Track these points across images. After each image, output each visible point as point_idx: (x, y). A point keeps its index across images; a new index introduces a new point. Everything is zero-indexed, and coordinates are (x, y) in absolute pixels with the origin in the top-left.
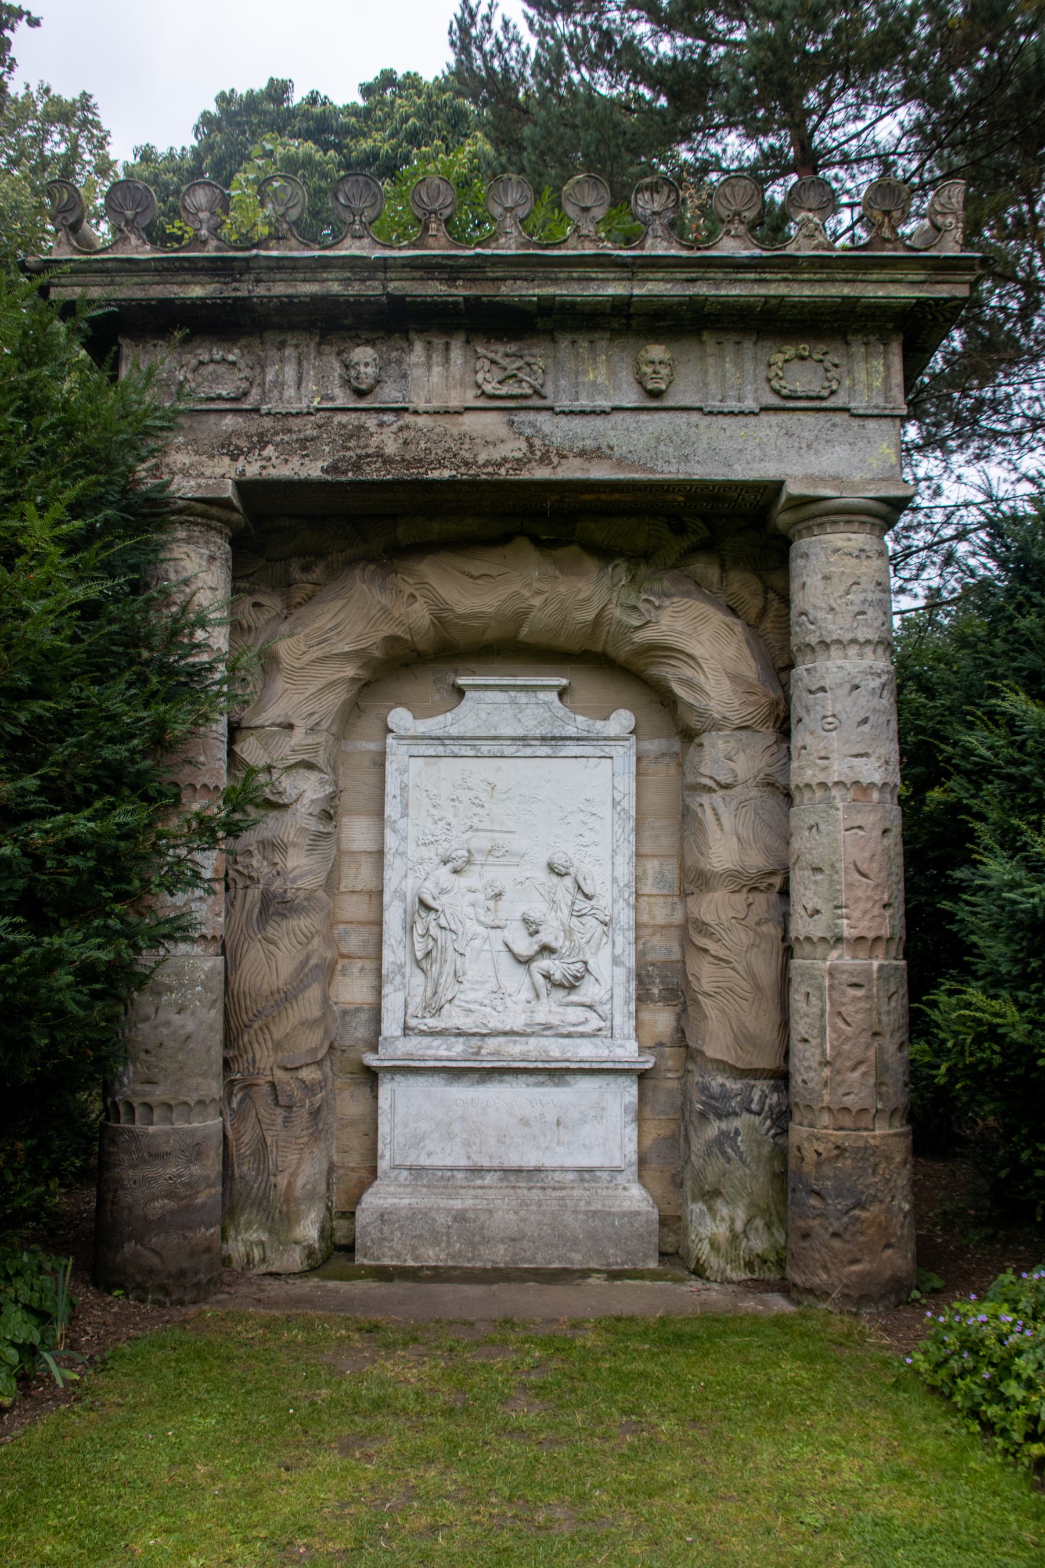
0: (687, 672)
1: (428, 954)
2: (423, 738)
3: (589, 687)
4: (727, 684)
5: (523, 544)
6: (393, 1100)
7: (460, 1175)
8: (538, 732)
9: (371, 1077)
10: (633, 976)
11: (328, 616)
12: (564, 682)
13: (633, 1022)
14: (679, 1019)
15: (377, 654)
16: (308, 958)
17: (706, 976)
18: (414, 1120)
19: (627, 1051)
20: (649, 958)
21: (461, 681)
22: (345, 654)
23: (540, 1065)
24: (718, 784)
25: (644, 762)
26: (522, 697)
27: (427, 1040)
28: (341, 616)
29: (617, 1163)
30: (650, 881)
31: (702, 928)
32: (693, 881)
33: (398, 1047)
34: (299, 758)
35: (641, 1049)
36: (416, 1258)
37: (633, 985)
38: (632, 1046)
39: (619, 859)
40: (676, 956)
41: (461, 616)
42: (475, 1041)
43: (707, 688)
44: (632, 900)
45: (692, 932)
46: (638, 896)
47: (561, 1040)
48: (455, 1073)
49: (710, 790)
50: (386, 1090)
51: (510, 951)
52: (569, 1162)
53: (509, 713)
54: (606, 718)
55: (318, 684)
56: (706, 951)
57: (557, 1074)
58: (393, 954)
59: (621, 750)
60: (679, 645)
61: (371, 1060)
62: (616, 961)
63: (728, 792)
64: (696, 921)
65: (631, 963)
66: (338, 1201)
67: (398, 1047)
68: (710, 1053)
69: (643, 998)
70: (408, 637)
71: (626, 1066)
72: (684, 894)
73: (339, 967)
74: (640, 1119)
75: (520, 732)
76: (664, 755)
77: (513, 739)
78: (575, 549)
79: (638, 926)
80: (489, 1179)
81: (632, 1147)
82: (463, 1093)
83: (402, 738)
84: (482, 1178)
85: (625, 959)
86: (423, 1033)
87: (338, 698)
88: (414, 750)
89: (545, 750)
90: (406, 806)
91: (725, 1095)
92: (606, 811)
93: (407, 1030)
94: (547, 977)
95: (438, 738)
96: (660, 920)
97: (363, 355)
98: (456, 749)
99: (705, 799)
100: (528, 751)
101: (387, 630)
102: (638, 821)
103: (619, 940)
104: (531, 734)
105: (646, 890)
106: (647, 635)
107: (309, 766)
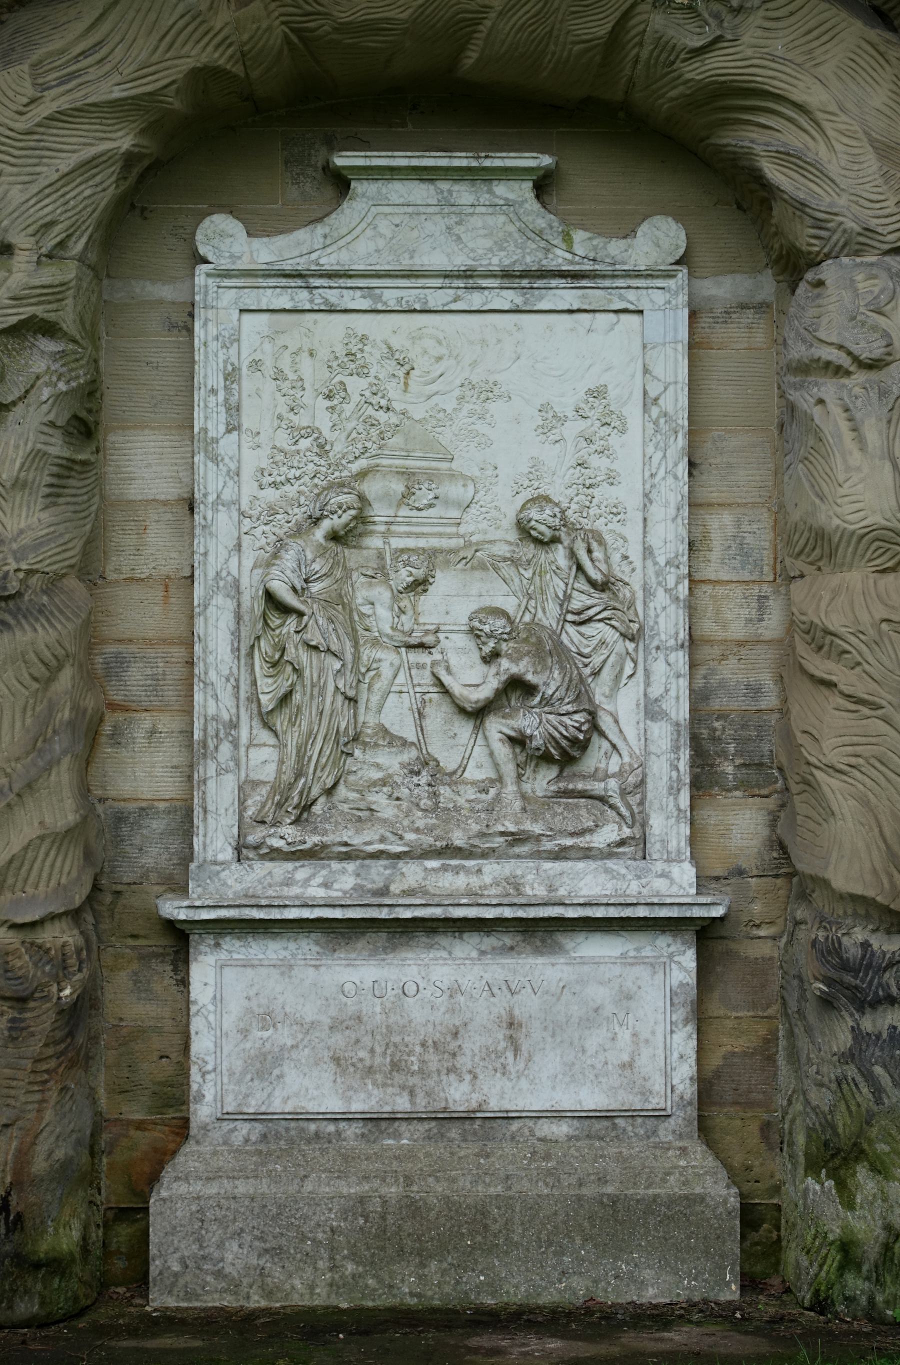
0: (792, 138)
1: (285, 698)
2: (267, 274)
4: (871, 163)
6: (219, 986)
7: (351, 1131)
8: (496, 262)
9: (179, 939)
10: (685, 739)
11: (80, 27)
12: (546, 160)
13: (686, 830)
14: (773, 823)
15: (176, 104)
16: (51, 709)
17: (831, 733)
19: (673, 883)
20: (716, 704)
21: (342, 160)
22: (114, 104)
23: (508, 913)
24: (856, 359)
25: (705, 321)
26: (464, 193)
27: (280, 869)
28: (105, 27)
29: (656, 1102)
30: (715, 555)
31: (821, 639)
32: (807, 548)
33: (224, 880)
34: (27, 312)
35: (703, 882)
36: (269, 1294)
37: (685, 755)
38: (685, 874)
39: (657, 512)
40: (770, 700)
41: (342, 28)
42: (378, 871)
43: (833, 169)
44: (683, 590)
45: (802, 648)
46: (694, 583)
47: (547, 865)
48: (339, 932)
49: (839, 371)
50: (205, 969)
51: (445, 691)
52: (566, 1100)
53: (436, 226)
54: (630, 233)
55: (65, 163)
56: (830, 685)
58: (215, 700)
59: (659, 297)
60: (778, 86)
61: (174, 909)
62: (651, 710)
63: (873, 375)
64: (810, 629)
65: (682, 711)
66: (110, 1192)
67: (224, 880)
68: (839, 883)
69: (703, 782)
70: (238, 70)
71: (674, 913)
72: (786, 578)
73: (107, 729)
74: (701, 1018)
75: (460, 261)
76: (743, 306)
77: (447, 275)
79: (694, 643)
80: (407, 1137)
81: (684, 1073)
83: (226, 274)
84: (397, 1136)
85: (668, 705)
86: (275, 855)
87: (102, 190)
88: (250, 299)
89: (507, 298)
90: (234, 409)
91: (869, 963)
94: (518, 741)
95: (299, 275)
96: (737, 630)
98: (333, 296)
99: (828, 388)
100: (476, 300)
101: (198, 55)
102: (695, 432)
103: (659, 668)
104: (483, 264)
105: (709, 572)
106: (717, 65)
107: (49, 329)
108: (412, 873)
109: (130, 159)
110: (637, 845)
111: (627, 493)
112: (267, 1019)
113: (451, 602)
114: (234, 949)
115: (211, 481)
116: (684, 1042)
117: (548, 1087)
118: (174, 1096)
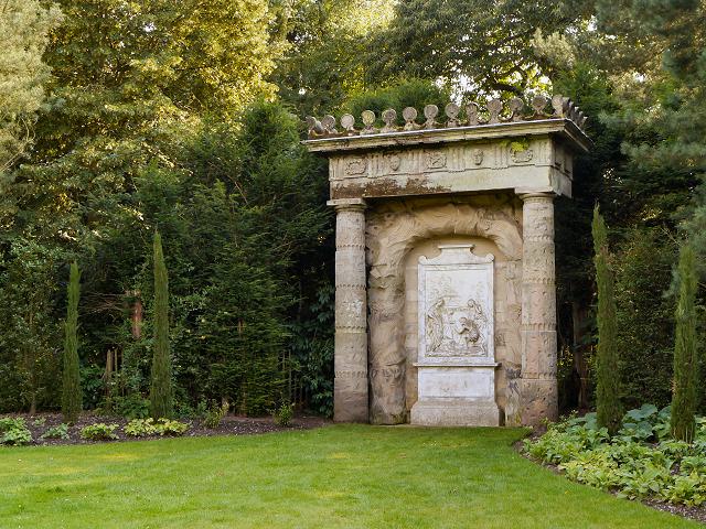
3: (480, 246)
5: (451, 205)
18: (428, 384)
26: (459, 251)
50: (420, 372)
52: (474, 394)
57: (470, 368)
58: (421, 332)
61: (415, 365)
65: (492, 333)
78: (467, 206)
82: (443, 374)
87: (401, 254)
92: (486, 286)
93: (426, 356)
97: (394, 159)
108: (451, 359)
109: (405, 249)
110: (486, 354)
111: (485, 298)
112: (429, 381)
113: (457, 316)
114: (424, 370)
115: (420, 298)
116: (493, 386)
117: (471, 393)
118: (417, 393)
